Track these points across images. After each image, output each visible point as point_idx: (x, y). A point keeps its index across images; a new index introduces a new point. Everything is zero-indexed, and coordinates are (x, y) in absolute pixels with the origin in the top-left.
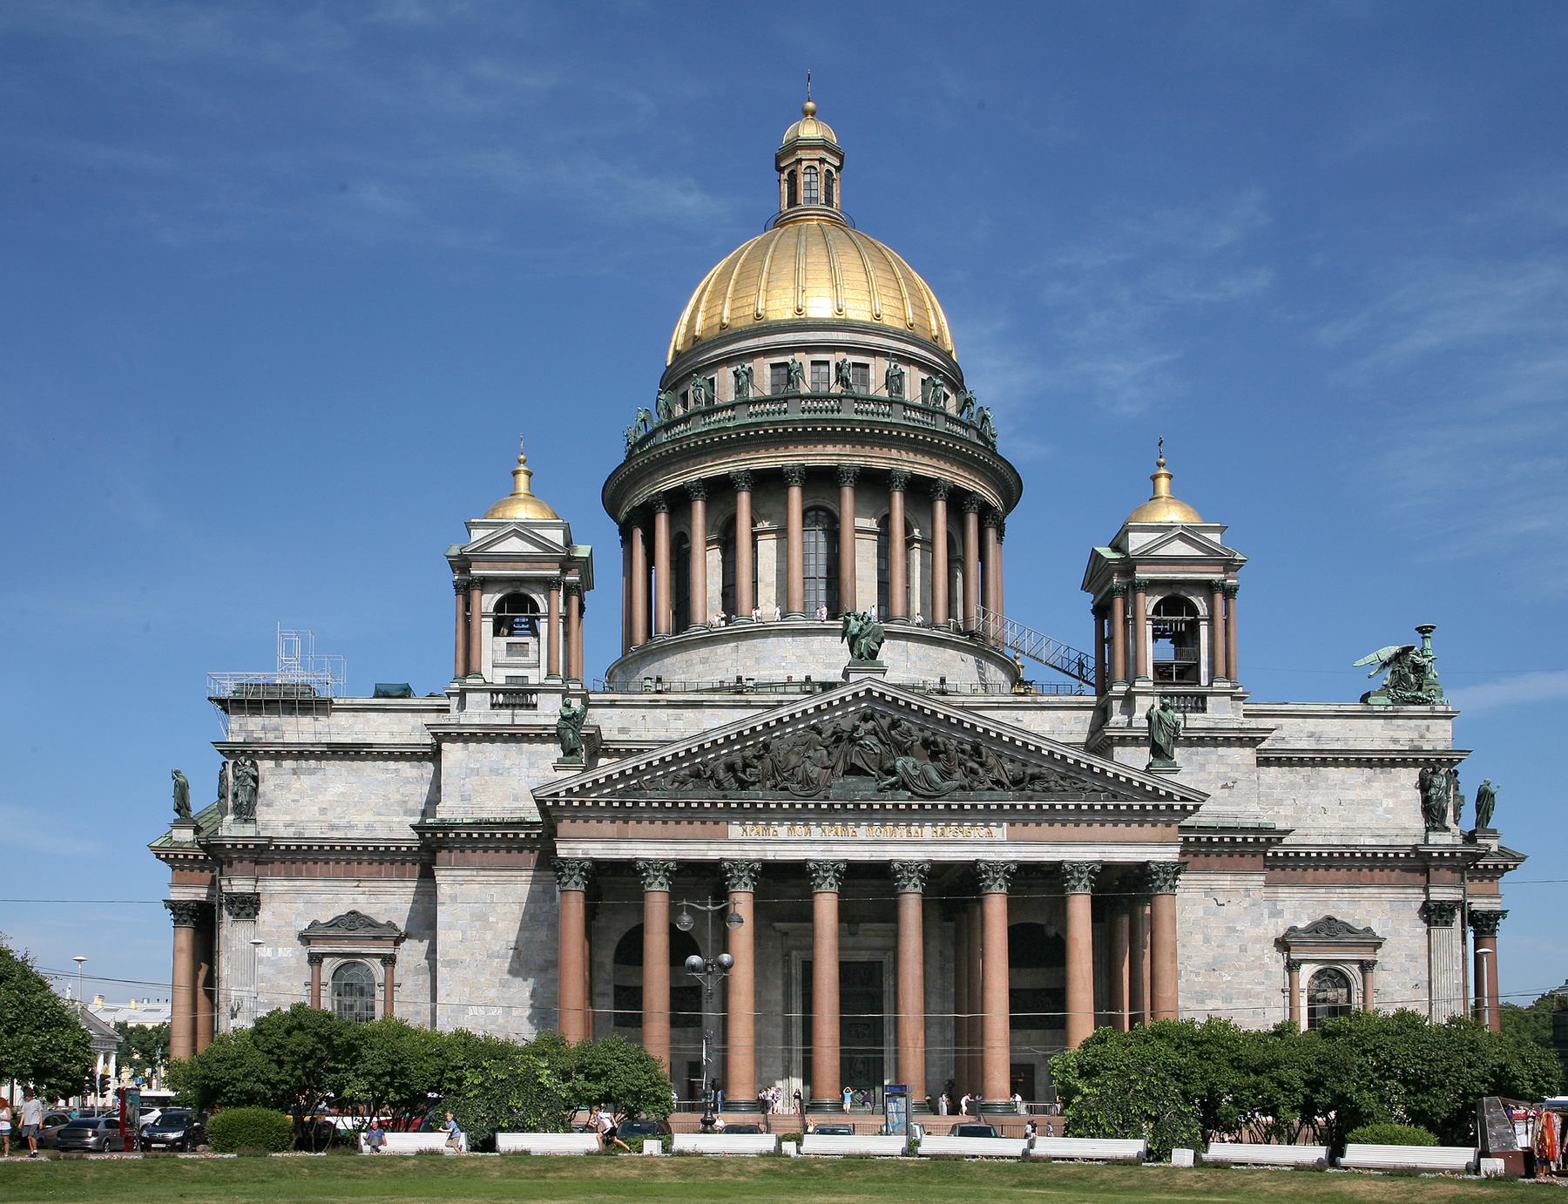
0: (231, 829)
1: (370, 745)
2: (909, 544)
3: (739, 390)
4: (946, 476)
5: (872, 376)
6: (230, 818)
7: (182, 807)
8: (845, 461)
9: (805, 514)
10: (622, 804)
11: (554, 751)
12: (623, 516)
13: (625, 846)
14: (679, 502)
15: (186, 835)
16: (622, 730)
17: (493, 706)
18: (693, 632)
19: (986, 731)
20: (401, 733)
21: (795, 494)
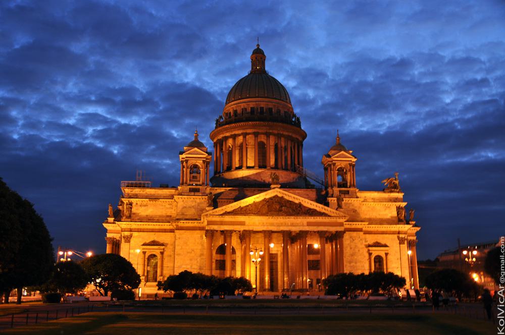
8: (268, 131)
12: (215, 141)
17: (190, 191)
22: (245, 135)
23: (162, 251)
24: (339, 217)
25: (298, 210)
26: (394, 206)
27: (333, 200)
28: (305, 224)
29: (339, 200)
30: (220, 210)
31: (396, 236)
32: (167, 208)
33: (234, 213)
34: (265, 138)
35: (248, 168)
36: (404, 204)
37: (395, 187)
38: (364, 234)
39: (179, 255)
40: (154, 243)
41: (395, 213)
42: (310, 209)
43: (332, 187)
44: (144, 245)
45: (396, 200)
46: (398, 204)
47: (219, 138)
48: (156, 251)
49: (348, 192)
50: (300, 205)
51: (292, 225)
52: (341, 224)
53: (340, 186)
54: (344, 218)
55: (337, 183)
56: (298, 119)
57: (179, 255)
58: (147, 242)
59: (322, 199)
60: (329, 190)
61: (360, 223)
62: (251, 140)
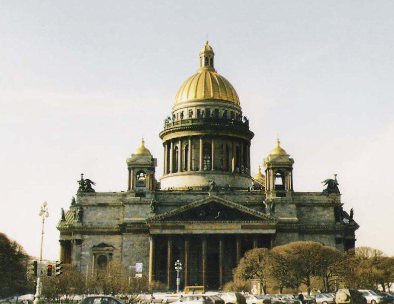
0: (76, 223)
1: (108, 204)
2: (227, 151)
3: (190, 116)
4: (236, 136)
5: (219, 111)
6: (76, 221)
7: (63, 217)
8: (213, 134)
9: (203, 145)
10: (164, 222)
11: (150, 210)
13: (164, 231)
14: (175, 140)
15: (64, 223)
16: (163, 200)
18: (179, 173)
19: (236, 206)
20: (114, 201)
21: (201, 140)
23: (111, 252)
28: (239, 226)
31: (333, 236)
32: (116, 212)
38: (299, 235)
39: (125, 256)
40: (103, 245)
42: (244, 213)
44: (94, 246)
47: (167, 139)
48: (105, 252)
54: (274, 221)
55: (275, 187)
56: (245, 118)
57: (125, 256)
58: (97, 244)
61: (295, 225)
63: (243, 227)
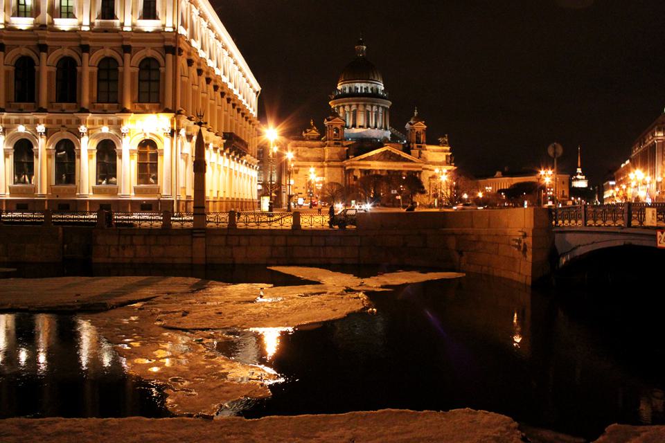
22: (358, 105)
24: (420, 163)
25: (399, 159)
26: (444, 154)
27: (415, 152)
29: (420, 153)
30: (358, 158)
33: (365, 159)
34: (370, 107)
35: (360, 127)
36: (450, 154)
37: (446, 143)
41: (444, 159)
42: (405, 158)
43: (413, 144)
45: (445, 151)
46: (447, 153)
49: (421, 147)
50: (400, 156)
51: (395, 167)
52: (421, 167)
53: (417, 143)
59: (407, 150)
60: (411, 145)
62: (361, 108)
63: (404, 166)
